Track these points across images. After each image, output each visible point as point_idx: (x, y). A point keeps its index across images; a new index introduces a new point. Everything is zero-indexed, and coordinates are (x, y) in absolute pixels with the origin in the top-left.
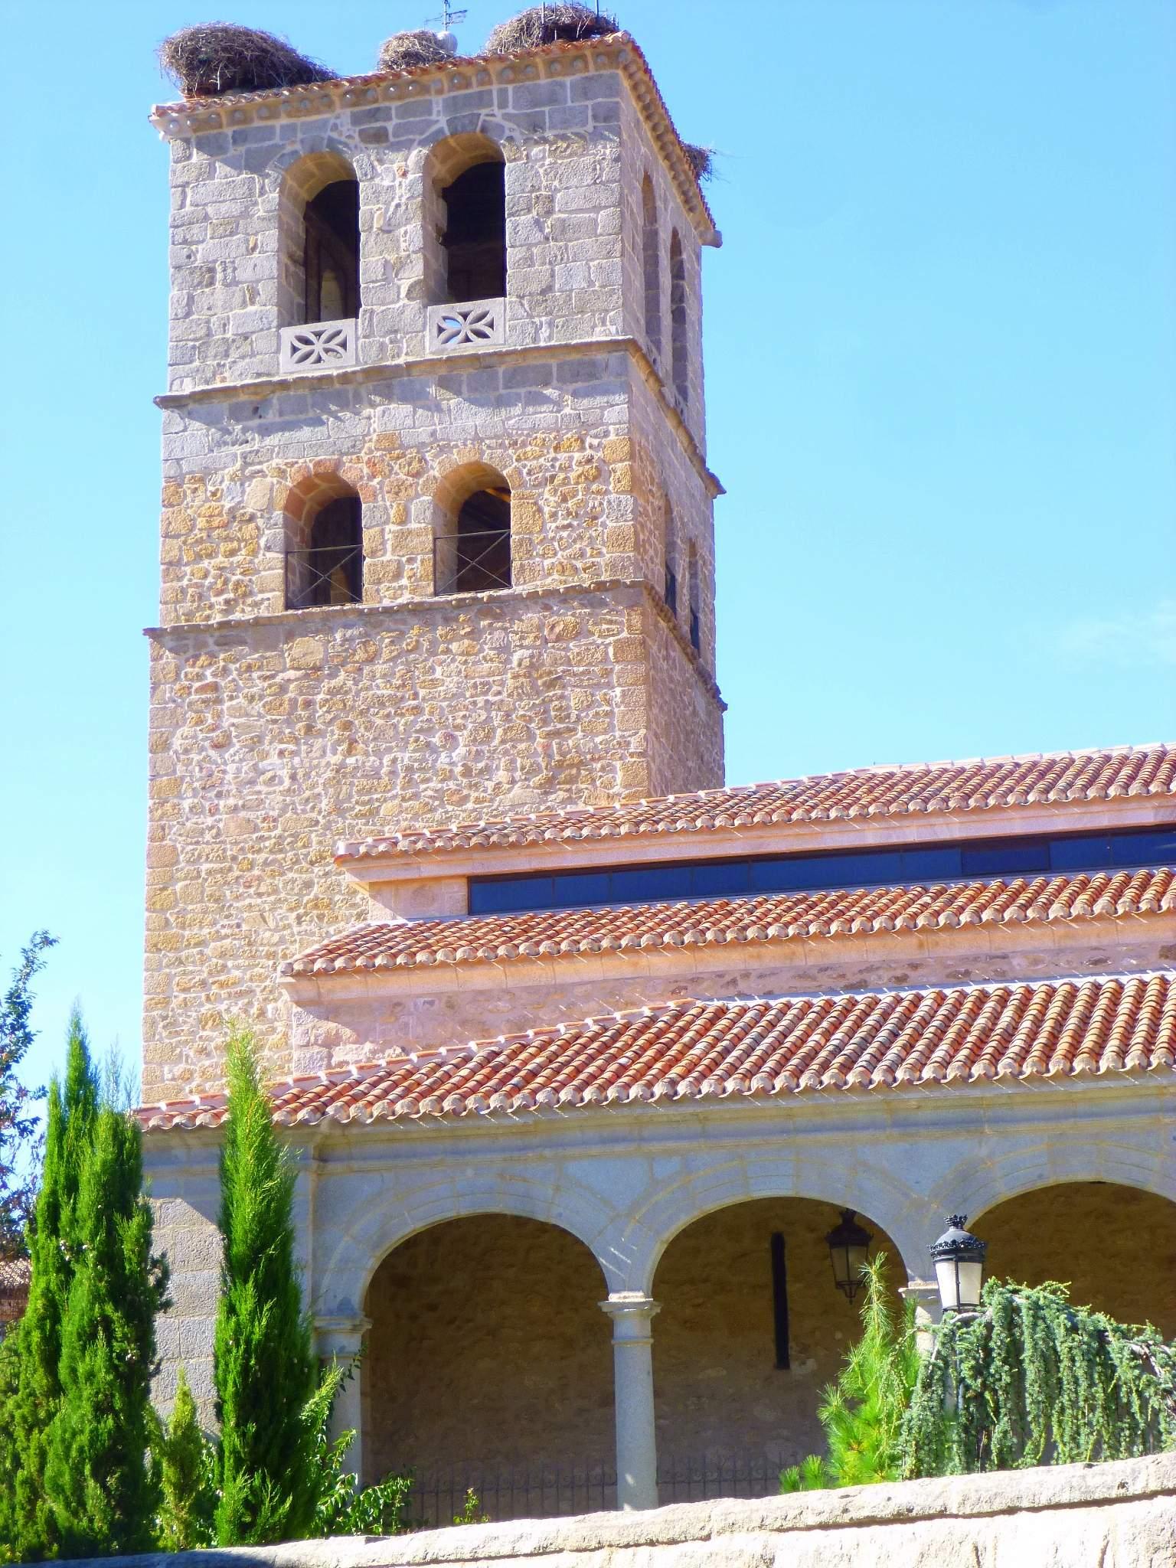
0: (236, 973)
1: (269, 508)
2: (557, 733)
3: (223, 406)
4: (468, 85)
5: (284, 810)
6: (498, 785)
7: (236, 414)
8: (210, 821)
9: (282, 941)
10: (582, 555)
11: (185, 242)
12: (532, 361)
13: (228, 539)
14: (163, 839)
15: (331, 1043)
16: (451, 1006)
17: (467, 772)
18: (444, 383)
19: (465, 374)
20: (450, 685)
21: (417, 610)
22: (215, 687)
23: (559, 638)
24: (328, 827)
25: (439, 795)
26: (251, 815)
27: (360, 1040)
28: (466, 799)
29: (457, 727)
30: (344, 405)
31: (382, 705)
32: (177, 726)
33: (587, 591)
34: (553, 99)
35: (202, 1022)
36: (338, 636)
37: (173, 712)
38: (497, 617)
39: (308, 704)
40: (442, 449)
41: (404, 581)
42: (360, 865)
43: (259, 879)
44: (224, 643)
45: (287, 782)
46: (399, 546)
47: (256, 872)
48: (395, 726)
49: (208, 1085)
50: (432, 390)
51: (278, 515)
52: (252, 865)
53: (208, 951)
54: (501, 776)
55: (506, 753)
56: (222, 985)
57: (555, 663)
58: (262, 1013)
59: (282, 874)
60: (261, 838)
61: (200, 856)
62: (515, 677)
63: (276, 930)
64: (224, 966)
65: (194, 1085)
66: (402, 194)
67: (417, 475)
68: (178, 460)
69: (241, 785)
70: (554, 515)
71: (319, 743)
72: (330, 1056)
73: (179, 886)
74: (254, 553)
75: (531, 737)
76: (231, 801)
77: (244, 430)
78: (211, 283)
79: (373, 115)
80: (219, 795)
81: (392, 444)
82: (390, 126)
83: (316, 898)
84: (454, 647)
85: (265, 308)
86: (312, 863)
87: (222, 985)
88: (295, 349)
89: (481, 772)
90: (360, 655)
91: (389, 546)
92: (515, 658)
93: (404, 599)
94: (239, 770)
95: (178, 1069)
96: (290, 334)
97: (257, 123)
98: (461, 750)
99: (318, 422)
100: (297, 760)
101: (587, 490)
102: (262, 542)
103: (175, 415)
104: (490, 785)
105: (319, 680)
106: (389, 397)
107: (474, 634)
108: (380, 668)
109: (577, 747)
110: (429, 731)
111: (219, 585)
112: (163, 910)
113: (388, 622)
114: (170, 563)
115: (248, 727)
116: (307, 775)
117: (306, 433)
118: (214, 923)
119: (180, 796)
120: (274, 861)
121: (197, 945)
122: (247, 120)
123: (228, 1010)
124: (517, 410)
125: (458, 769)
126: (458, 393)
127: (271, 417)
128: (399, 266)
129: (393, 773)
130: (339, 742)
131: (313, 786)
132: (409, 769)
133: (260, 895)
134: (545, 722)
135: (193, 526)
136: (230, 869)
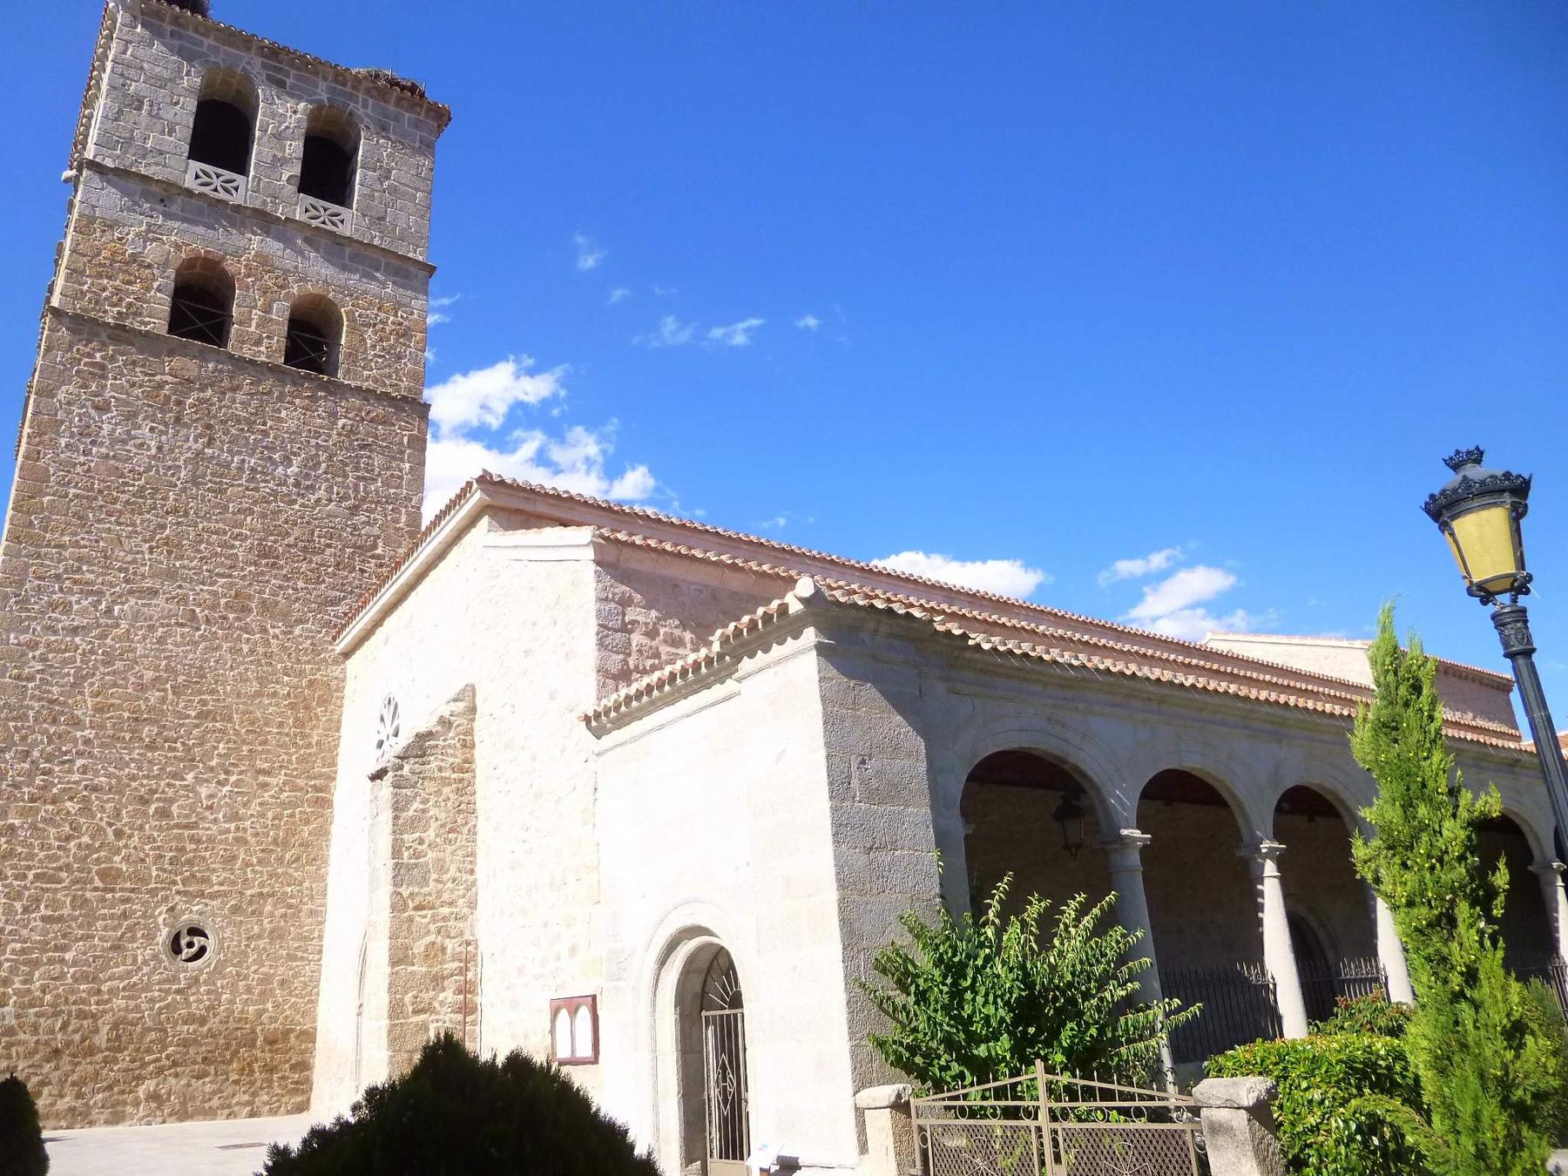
0: (92, 576)
1: (166, 264)
2: (363, 478)
3: (133, 185)
4: (344, 85)
5: (148, 470)
6: (318, 500)
7: (147, 196)
8: (82, 459)
9: (134, 561)
10: (390, 377)
11: (122, 75)
12: (369, 253)
13: (126, 272)
14: (38, 459)
15: (625, 602)
16: (714, 597)
17: (297, 484)
18: (306, 240)
19: (324, 241)
20: (291, 425)
21: (273, 369)
22: (103, 367)
23: (372, 421)
24: (184, 490)
25: (274, 493)
26: (120, 465)
27: (648, 607)
28: (295, 502)
29: (294, 454)
30: (233, 226)
31: (239, 422)
32: (63, 383)
33: (394, 398)
34: (396, 119)
35: (53, 606)
36: (211, 366)
37: (61, 373)
38: (331, 394)
39: (179, 403)
40: (301, 280)
41: (263, 349)
42: (492, 488)
43: (121, 513)
44: (115, 339)
45: (154, 451)
46: (258, 326)
47: (118, 506)
48: (247, 439)
49: (50, 656)
50: (299, 242)
51: (171, 272)
52: (115, 501)
53: (66, 554)
54: (322, 493)
55: (327, 480)
56: (75, 582)
57: (368, 434)
58: (109, 611)
59: (141, 514)
60: (126, 484)
61: (69, 482)
62: (339, 434)
63: (130, 552)
64: (79, 568)
65: (38, 653)
66: (292, 121)
67: (282, 287)
68: (94, 207)
69: (114, 441)
70: (374, 347)
71: (184, 432)
72: (624, 615)
73: (46, 499)
74: (148, 289)
75: (346, 476)
76: (103, 450)
77: (152, 209)
78: (139, 108)
79: (279, 70)
80: (93, 443)
81: (264, 260)
82: (289, 82)
83: (167, 537)
84: (297, 401)
85: (181, 140)
86: (167, 513)
87: (75, 582)
88: (197, 177)
89: (307, 488)
90: (226, 384)
91: (254, 323)
92: (341, 422)
93: (263, 358)
94: (114, 431)
95: (24, 638)
96: (195, 166)
97: (190, 33)
98: (294, 469)
99: (211, 227)
100: (164, 438)
101: (397, 340)
102: (155, 285)
103: (96, 177)
104: (313, 498)
105: (191, 390)
106: (267, 233)
107: (313, 398)
108: (239, 397)
109: (377, 491)
110: (272, 449)
111: (115, 299)
112: (29, 513)
113: (251, 369)
114: (74, 271)
115: (127, 404)
116: (171, 451)
117: (201, 230)
118: (76, 534)
119: (58, 433)
120: (134, 503)
121: (55, 547)
122: (185, 27)
123: (78, 602)
124: (357, 277)
125: (291, 480)
126: (317, 251)
127: (175, 208)
128: (284, 162)
129: (241, 469)
130: (201, 436)
131: (175, 460)
132: (253, 470)
133: (119, 524)
134: (357, 469)
135: (98, 254)
136: (96, 498)
